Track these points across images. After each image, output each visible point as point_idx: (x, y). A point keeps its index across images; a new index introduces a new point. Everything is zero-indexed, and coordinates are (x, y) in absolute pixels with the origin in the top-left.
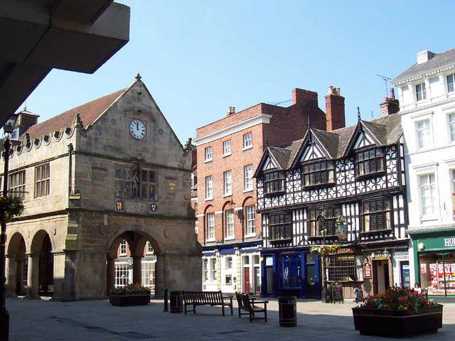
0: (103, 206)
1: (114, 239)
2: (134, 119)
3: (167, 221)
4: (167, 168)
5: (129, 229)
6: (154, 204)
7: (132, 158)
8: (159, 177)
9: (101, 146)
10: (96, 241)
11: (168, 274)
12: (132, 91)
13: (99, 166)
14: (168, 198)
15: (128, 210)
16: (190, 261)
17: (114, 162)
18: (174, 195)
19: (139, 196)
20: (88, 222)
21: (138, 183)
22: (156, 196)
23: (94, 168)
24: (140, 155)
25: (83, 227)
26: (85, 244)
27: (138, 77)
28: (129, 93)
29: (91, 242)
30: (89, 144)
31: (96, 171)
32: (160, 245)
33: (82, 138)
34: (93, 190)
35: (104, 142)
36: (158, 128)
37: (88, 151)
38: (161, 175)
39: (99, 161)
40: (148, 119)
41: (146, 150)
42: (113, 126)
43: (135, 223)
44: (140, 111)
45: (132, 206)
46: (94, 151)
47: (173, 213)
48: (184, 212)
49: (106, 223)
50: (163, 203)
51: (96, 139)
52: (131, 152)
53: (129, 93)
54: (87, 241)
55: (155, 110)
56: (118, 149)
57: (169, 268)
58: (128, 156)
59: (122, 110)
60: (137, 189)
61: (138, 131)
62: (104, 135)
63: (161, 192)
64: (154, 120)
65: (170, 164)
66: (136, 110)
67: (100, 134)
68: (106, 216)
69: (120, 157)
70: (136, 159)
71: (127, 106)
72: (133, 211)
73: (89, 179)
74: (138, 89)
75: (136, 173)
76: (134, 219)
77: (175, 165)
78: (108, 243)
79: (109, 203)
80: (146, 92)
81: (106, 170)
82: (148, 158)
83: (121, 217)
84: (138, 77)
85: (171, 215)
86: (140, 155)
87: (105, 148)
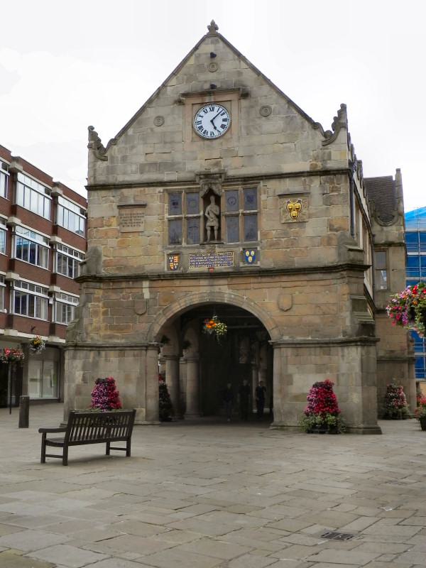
0: (139, 267)
1: (163, 321)
2: (202, 104)
3: (285, 278)
4: (280, 176)
5: (196, 300)
6: (250, 250)
7: (198, 175)
8: (263, 197)
9: (134, 168)
10: (127, 327)
11: (291, 383)
12: (198, 57)
13: (132, 202)
14: (286, 234)
15: (192, 269)
16: (343, 356)
17: (161, 189)
18: (302, 223)
19: (219, 238)
20: (114, 296)
21: (218, 217)
22: (259, 233)
23: (120, 207)
24: (217, 164)
25: (105, 305)
26: (109, 332)
27: (213, 27)
28: (192, 61)
29: (120, 329)
30: (110, 170)
31: (126, 212)
32: (269, 326)
33: (99, 163)
34: (122, 242)
35: (142, 159)
36: (259, 108)
37: (111, 180)
38: (267, 194)
39: (131, 195)
40: (234, 97)
41: (230, 153)
42: (158, 130)
43: (205, 290)
44: (213, 87)
45: (197, 259)
46: (121, 178)
47: (298, 262)
48: (329, 256)
49: (147, 294)
50: (272, 245)
51: (124, 159)
52: (197, 164)
53: (192, 61)
54: (112, 328)
55: (249, 80)
56: (171, 166)
57: (291, 369)
58: (190, 172)
59: (176, 97)
60: (216, 228)
61: (210, 120)
62: (141, 148)
63: (269, 224)
64: (245, 95)
65: (288, 168)
66: (207, 86)
67: (133, 147)
68: (146, 284)
69: (174, 177)
70: (207, 176)
71: (184, 88)
72: (205, 269)
73: (115, 225)
74: (209, 48)
75: (212, 198)
76: (203, 282)
77: (305, 166)
78: (150, 330)
79: (158, 262)
80: (228, 50)
81: (144, 206)
82: (235, 168)
83: (177, 283)
84: (213, 27)
85: (297, 266)
86: (217, 164)
87: (142, 169)
